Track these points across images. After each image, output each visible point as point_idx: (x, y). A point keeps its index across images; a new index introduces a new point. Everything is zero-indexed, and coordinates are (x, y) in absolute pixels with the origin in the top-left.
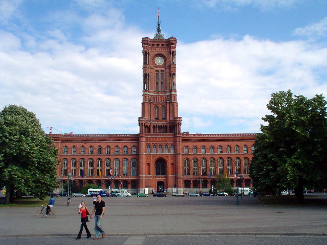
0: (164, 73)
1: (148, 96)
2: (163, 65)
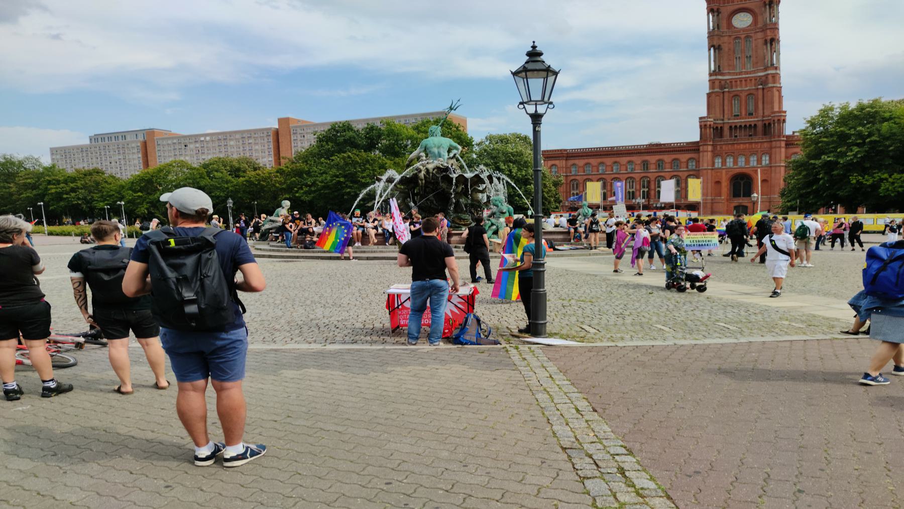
0: (754, 39)
1: (718, 81)
2: (750, 25)
